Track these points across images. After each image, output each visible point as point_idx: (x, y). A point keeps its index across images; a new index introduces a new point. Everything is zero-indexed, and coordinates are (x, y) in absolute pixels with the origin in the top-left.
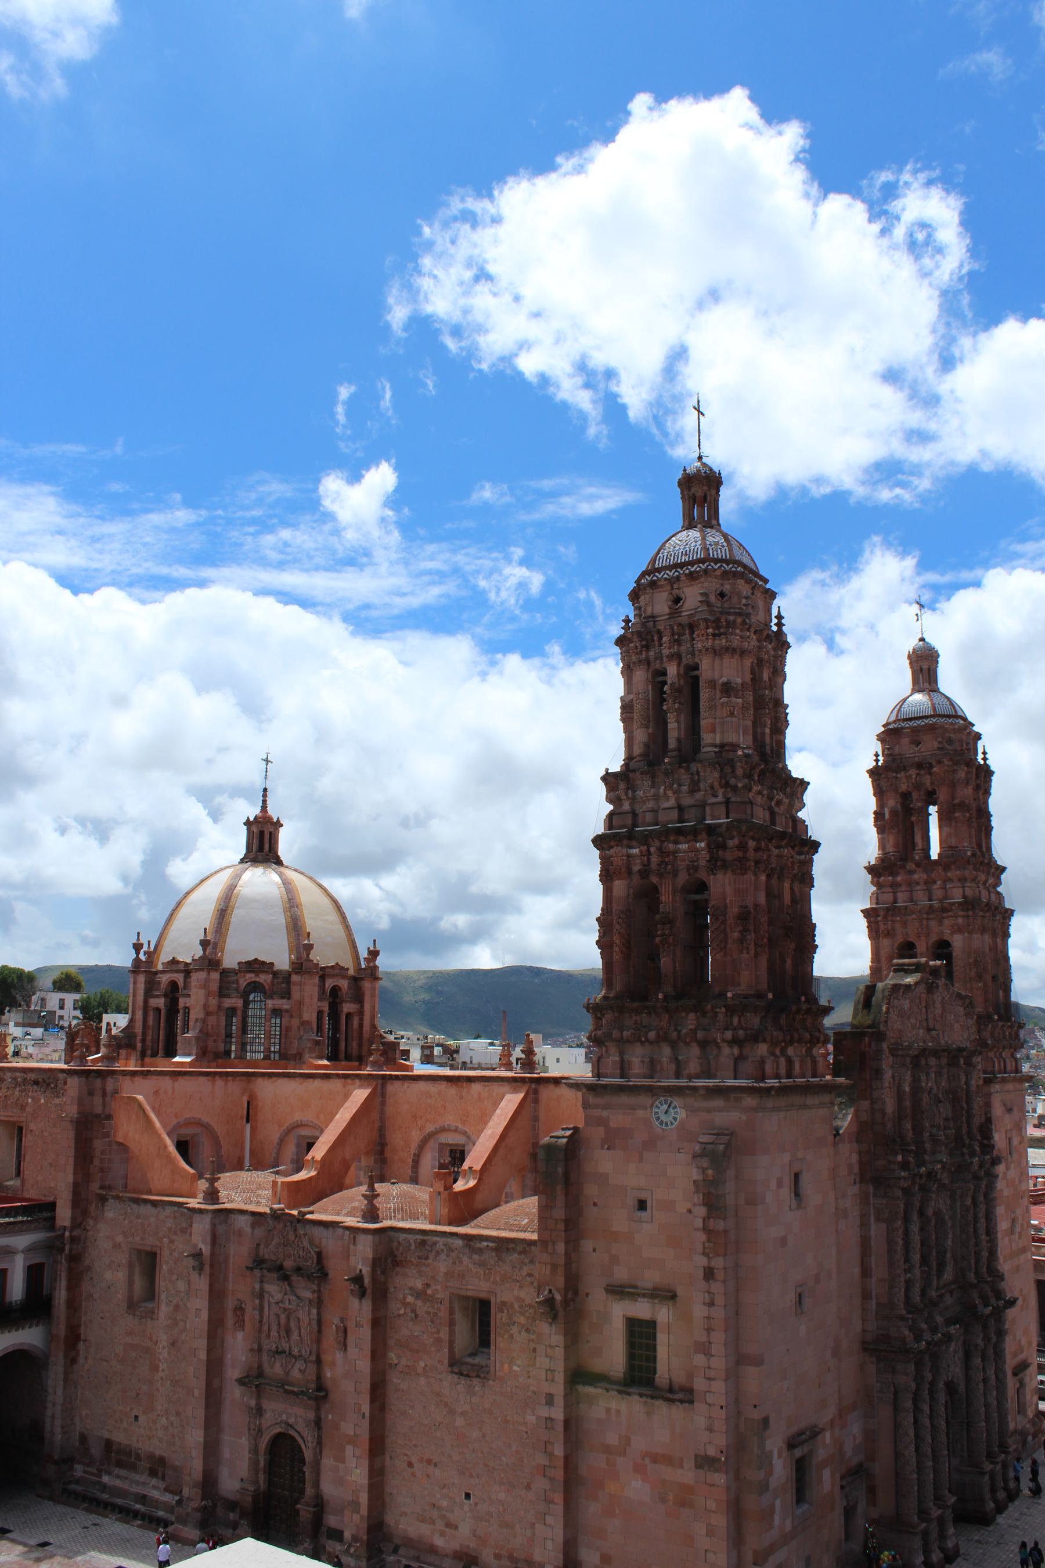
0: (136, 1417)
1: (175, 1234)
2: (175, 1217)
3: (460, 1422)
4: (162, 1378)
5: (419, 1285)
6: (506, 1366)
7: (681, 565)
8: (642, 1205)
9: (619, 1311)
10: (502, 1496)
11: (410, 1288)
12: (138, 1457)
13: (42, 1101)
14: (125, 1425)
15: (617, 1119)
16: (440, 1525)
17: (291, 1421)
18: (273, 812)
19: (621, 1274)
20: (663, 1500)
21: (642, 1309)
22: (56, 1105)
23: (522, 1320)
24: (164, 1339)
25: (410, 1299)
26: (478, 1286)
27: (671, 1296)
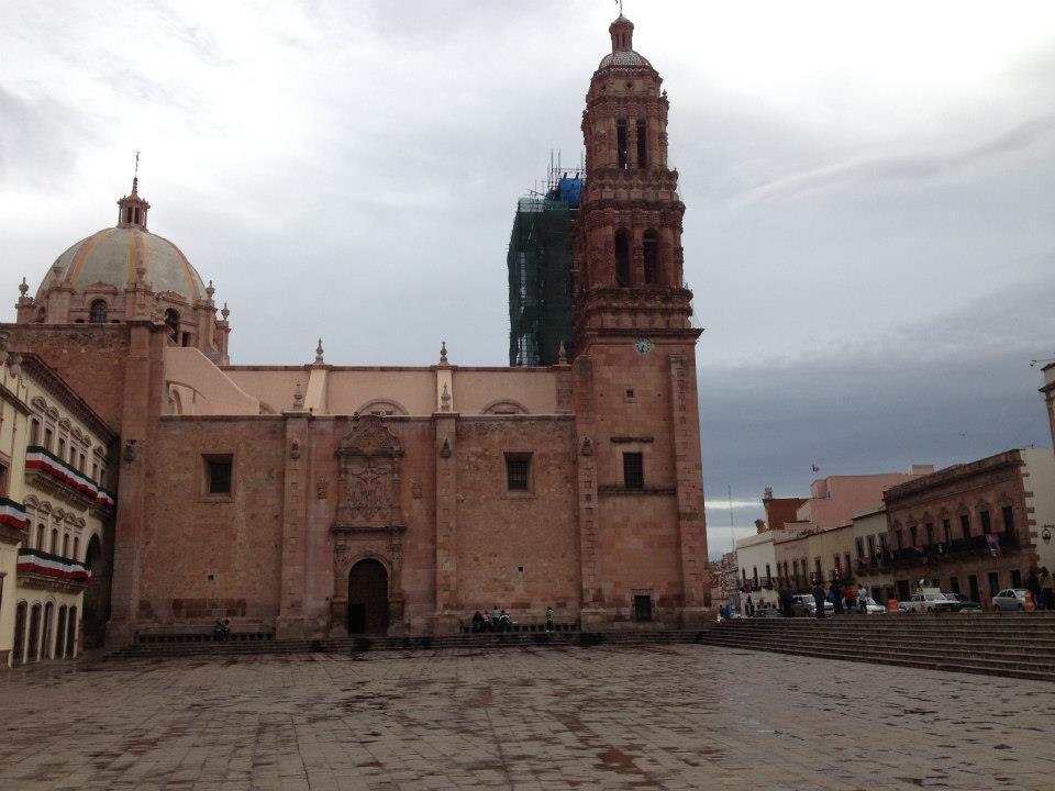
0: (211, 577)
1: (253, 439)
2: (252, 428)
3: (513, 526)
4: (240, 544)
5: (480, 450)
6: (546, 490)
7: (633, 67)
8: (630, 393)
9: (620, 450)
10: (545, 565)
11: (472, 453)
12: (215, 606)
13: (83, 351)
14: (197, 585)
15: (614, 350)
16: (500, 591)
17: (374, 550)
18: (141, 195)
19: (619, 432)
20: (651, 546)
21: (633, 448)
22: (102, 354)
23: (556, 462)
24: (241, 515)
25: (472, 460)
26: (521, 446)
27: (650, 440)
